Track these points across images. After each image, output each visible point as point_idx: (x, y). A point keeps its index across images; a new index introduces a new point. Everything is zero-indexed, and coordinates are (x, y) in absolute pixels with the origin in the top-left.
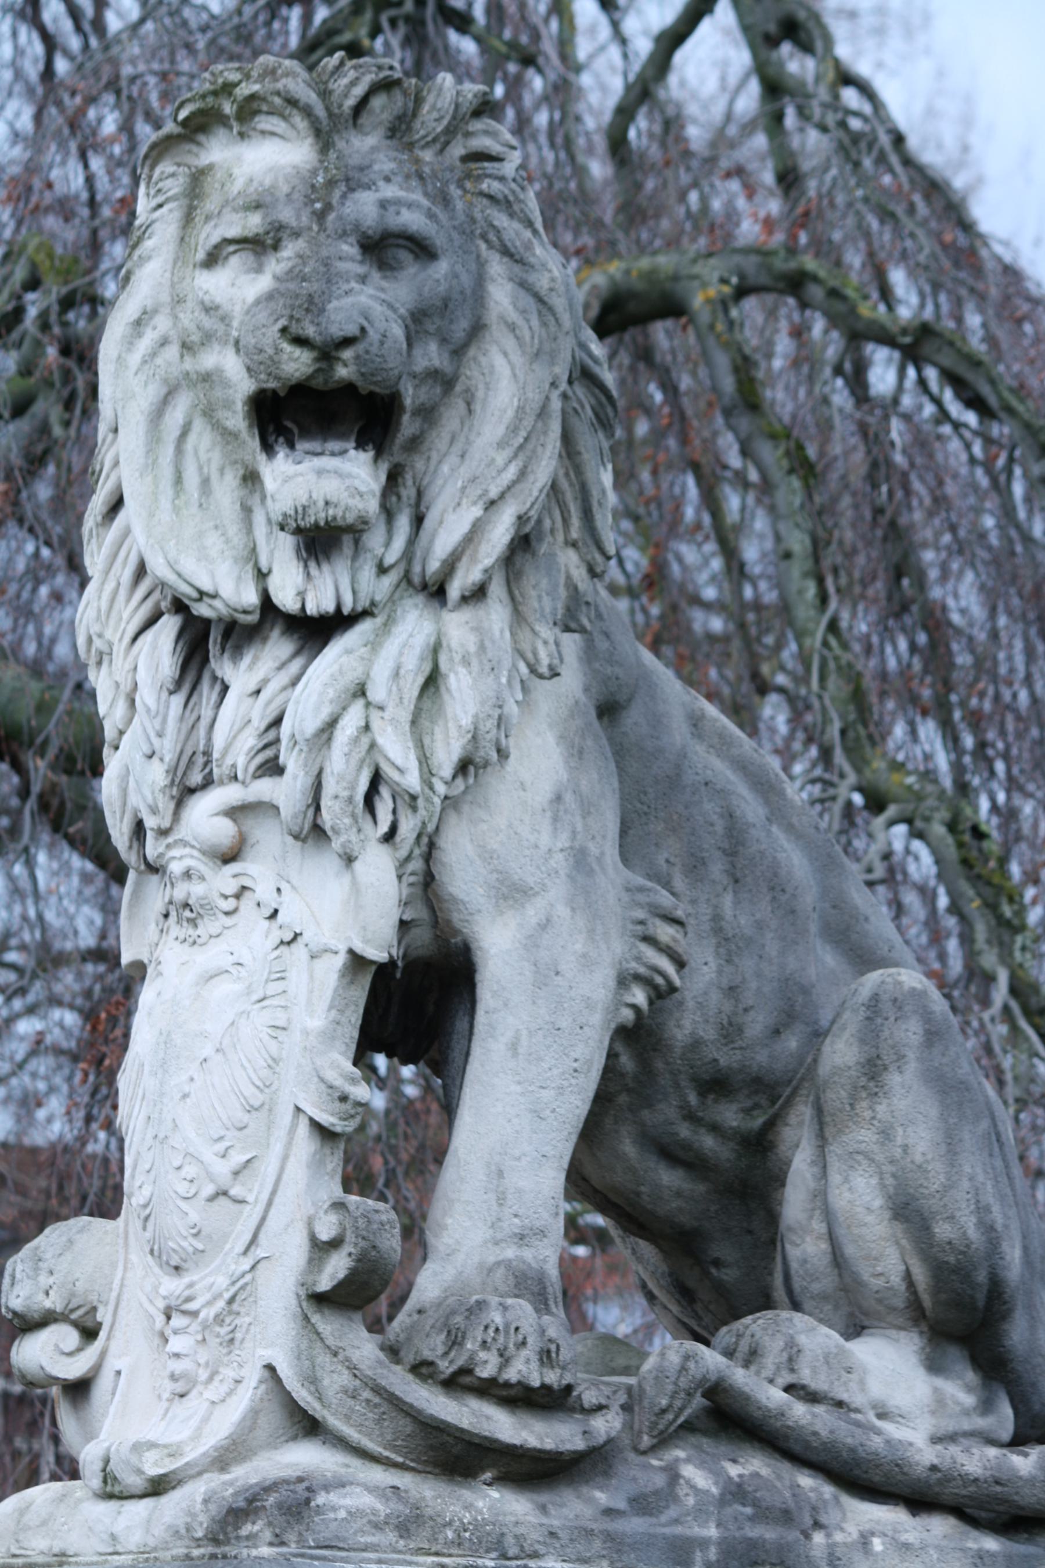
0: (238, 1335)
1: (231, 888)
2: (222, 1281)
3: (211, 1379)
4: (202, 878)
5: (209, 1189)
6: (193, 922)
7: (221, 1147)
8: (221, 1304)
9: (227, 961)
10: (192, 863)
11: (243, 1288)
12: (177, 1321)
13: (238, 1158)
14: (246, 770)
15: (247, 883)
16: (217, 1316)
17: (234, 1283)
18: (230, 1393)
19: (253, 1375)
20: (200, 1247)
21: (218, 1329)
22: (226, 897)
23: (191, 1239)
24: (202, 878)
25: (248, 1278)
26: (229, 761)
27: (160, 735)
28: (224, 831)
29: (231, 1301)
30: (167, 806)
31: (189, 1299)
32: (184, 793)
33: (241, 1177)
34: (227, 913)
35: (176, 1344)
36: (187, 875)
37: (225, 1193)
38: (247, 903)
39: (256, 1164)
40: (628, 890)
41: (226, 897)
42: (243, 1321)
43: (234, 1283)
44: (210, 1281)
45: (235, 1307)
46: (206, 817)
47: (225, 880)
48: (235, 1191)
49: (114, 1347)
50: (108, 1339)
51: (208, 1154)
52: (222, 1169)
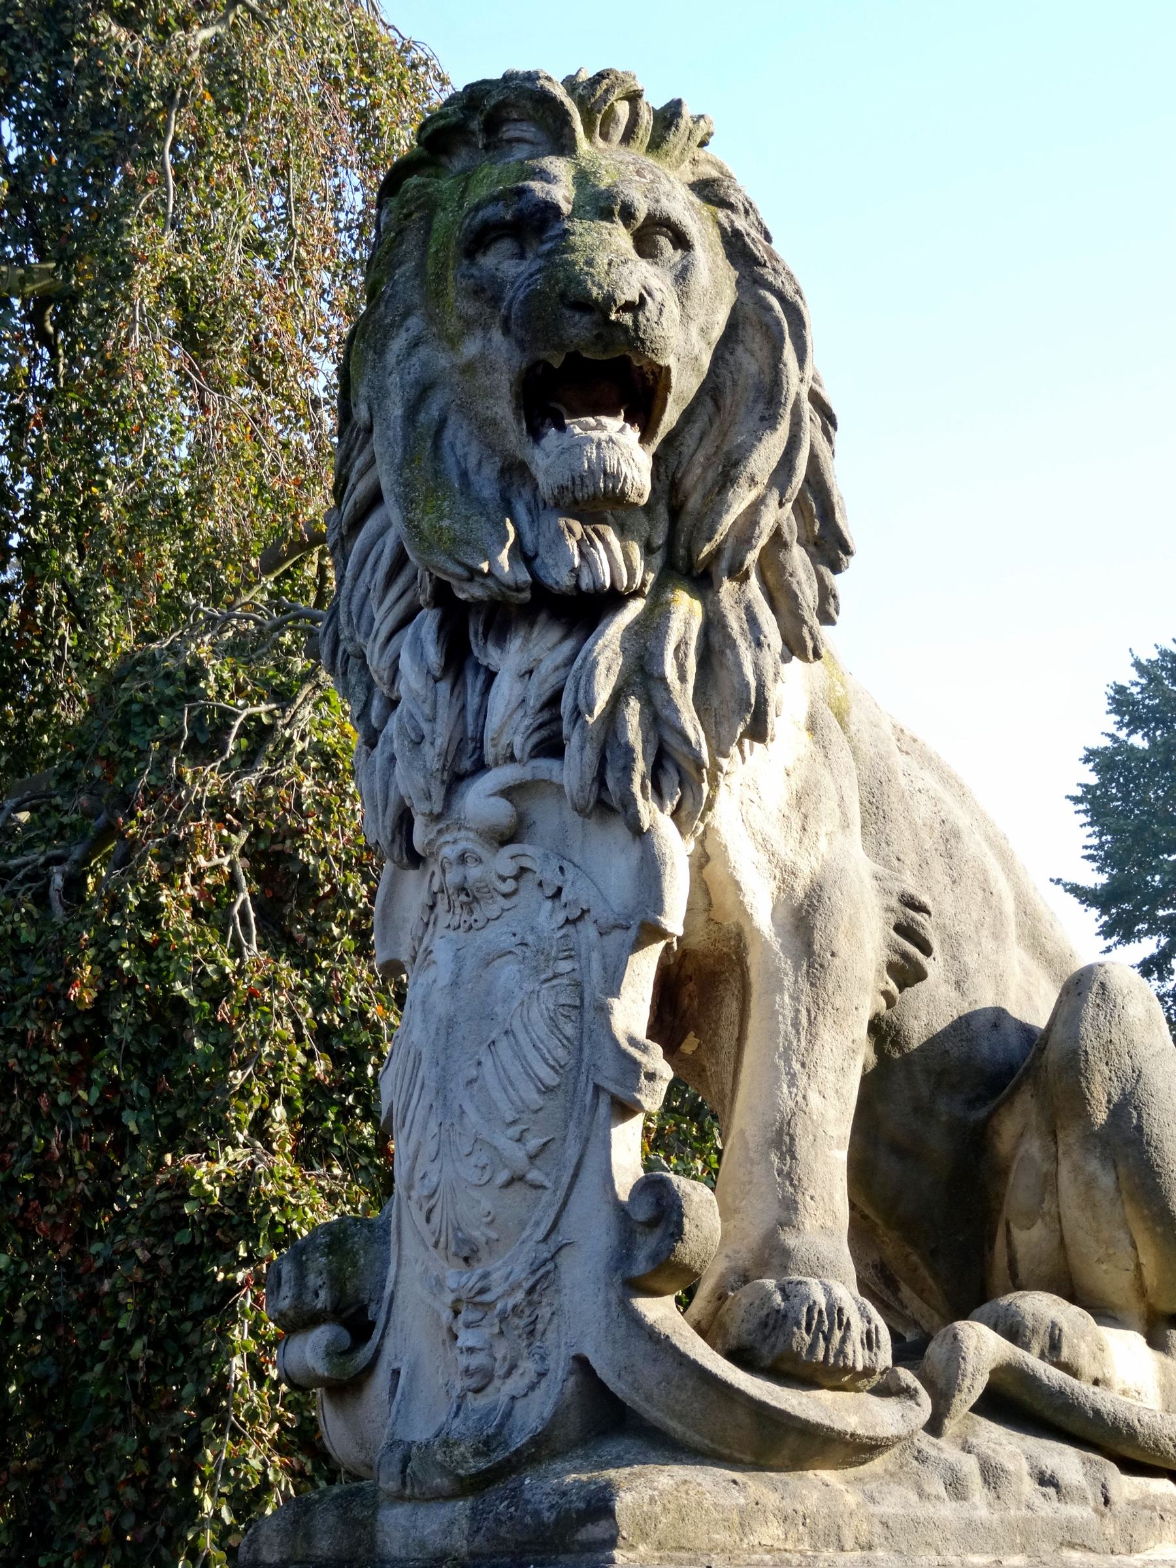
0: (540, 1327)
1: (509, 868)
2: (520, 1270)
3: (509, 1374)
4: (479, 860)
5: (503, 1176)
6: (468, 907)
7: (515, 1131)
8: (520, 1296)
9: (508, 942)
10: (470, 846)
11: (546, 1275)
12: (467, 1315)
13: (533, 1143)
14: (523, 750)
15: (527, 863)
16: (515, 1307)
17: (533, 1272)
18: (532, 1387)
19: (559, 1365)
20: (494, 1235)
21: (516, 1321)
22: (503, 879)
23: (483, 1228)
24: (479, 860)
25: (550, 1266)
26: (504, 741)
27: (432, 720)
28: (501, 812)
29: (531, 1291)
30: (438, 793)
31: (482, 1291)
32: (455, 781)
33: (538, 1162)
34: (505, 896)
35: (467, 1338)
36: (462, 859)
37: (521, 1178)
38: (529, 882)
39: (553, 1146)
40: (876, 878)
41: (503, 879)
42: (545, 1312)
43: (533, 1272)
44: (506, 1271)
45: (535, 1297)
46: (481, 800)
47: (503, 861)
48: (534, 1175)
49: (389, 1346)
50: (383, 1337)
51: (503, 1141)
52: (518, 1155)
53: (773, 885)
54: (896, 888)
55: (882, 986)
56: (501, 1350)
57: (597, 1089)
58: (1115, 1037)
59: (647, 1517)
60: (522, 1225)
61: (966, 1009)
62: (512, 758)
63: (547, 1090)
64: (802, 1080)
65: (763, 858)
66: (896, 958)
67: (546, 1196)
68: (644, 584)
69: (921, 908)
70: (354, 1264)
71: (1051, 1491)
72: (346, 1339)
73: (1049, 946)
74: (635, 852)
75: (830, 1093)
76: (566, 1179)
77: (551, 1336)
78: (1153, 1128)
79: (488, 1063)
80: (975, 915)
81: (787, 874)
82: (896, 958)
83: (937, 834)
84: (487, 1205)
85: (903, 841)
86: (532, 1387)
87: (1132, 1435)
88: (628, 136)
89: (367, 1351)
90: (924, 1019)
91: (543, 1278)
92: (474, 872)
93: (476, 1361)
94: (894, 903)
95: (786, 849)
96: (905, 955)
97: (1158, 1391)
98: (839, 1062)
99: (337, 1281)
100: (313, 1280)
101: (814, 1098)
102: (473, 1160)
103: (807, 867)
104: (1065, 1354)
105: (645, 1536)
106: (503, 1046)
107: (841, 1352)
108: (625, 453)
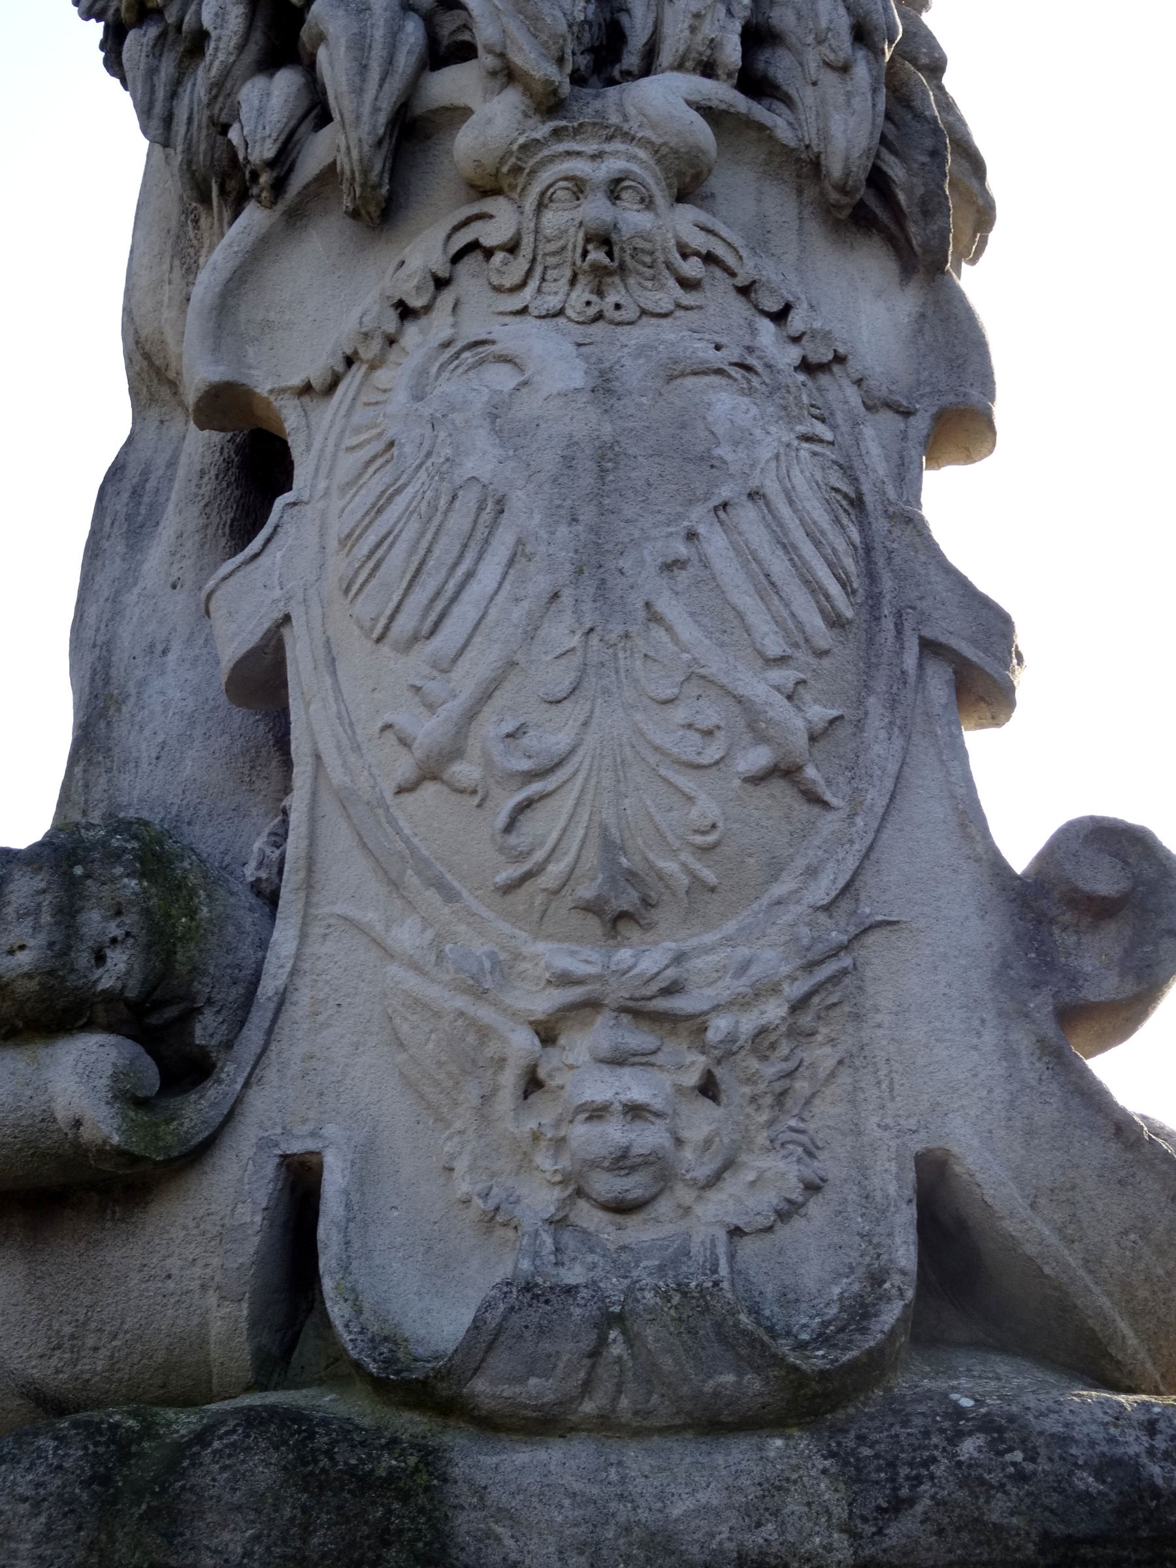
0: (802, 1086)
3: (714, 1181)
4: (647, 203)
5: (758, 758)
6: (600, 277)
7: (786, 676)
8: (774, 1011)
10: (635, 167)
11: (834, 979)
12: (582, 1044)
13: (819, 713)
16: (763, 1031)
17: (810, 966)
20: (709, 876)
21: (754, 1064)
23: (686, 856)
25: (846, 961)
29: (798, 1006)
31: (672, 990)
36: (615, 189)
42: (821, 1055)
43: (810, 966)
45: (806, 1020)
51: (759, 687)
52: (795, 723)
56: (701, 1121)
57: (929, 647)
60: (775, 869)
62: (708, 69)
63: (836, 622)
67: (829, 823)
70: (192, 913)
72: (150, 1076)
74: (906, 303)
76: (876, 797)
77: (827, 1113)
79: (716, 543)
84: (707, 808)
86: (787, 1212)
89: (197, 1110)
91: (828, 984)
92: (633, 219)
93: (648, 1138)
99: (161, 939)
100: (95, 922)
102: (680, 714)
106: (747, 516)
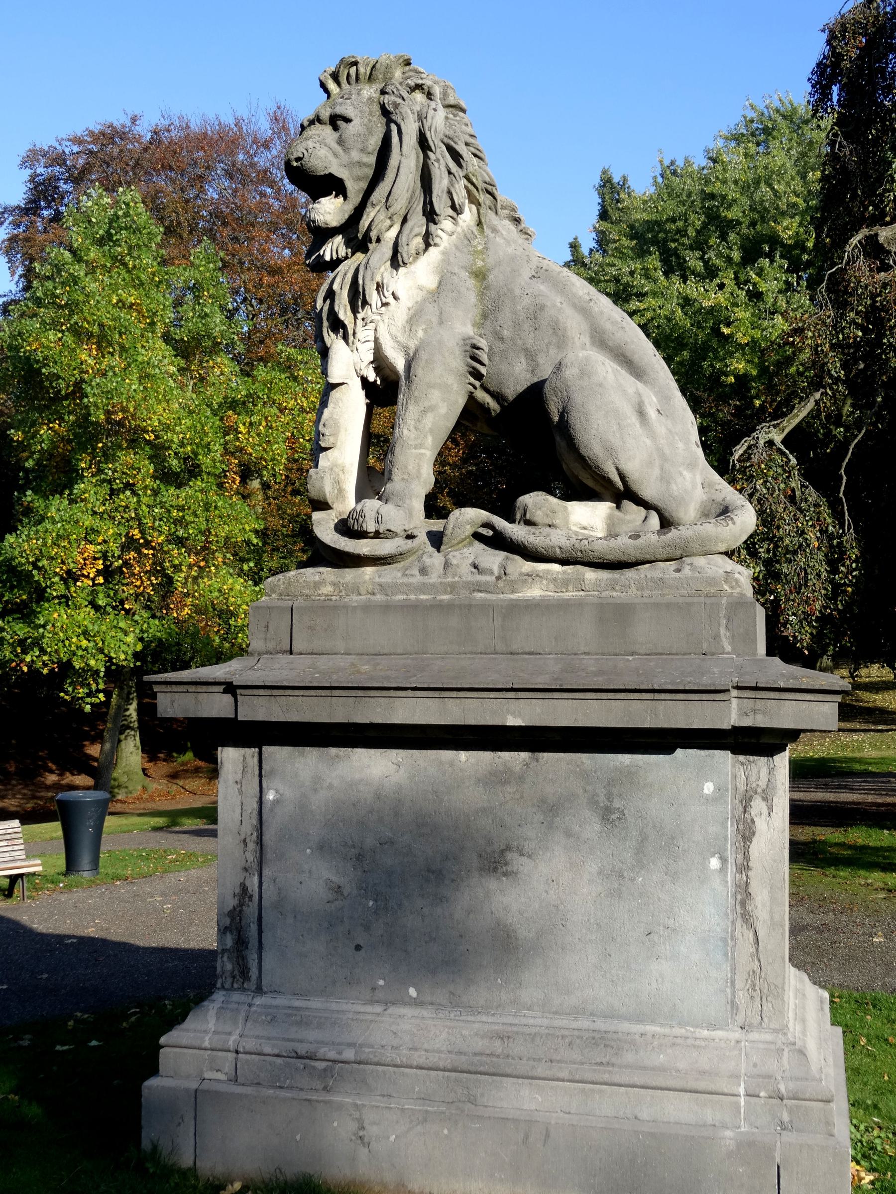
53: (402, 354)
54: (469, 342)
55: (467, 381)
58: (558, 385)
59: (276, 586)
61: (536, 380)
64: (402, 426)
65: (396, 345)
66: (471, 369)
68: (347, 254)
69: (478, 348)
71: (476, 570)
73: (610, 343)
75: (411, 428)
78: (572, 421)
80: (546, 341)
81: (405, 348)
82: (471, 369)
83: (531, 311)
85: (505, 318)
87: (525, 547)
88: (357, 79)
90: (512, 388)
94: (468, 348)
95: (403, 339)
96: (473, 368)
97: (605, 526)
98: (417, 417)
101: (405, 432)
103: (412, 344)
104: (528, 516)
105: (274, 592)
107: (361, 526)
108: (329, 210)
